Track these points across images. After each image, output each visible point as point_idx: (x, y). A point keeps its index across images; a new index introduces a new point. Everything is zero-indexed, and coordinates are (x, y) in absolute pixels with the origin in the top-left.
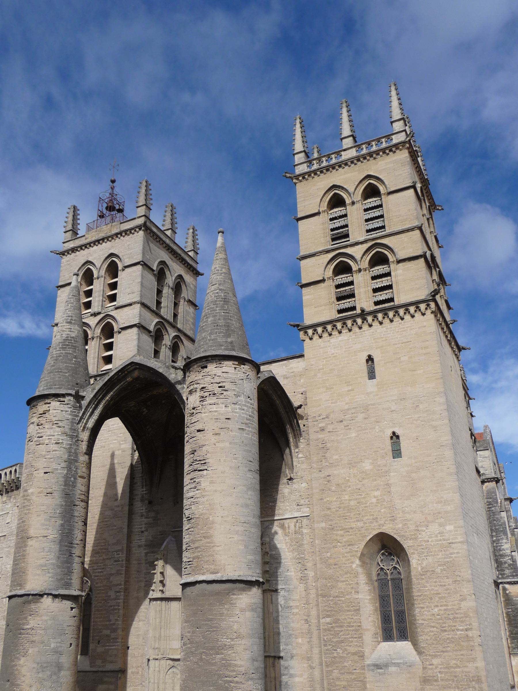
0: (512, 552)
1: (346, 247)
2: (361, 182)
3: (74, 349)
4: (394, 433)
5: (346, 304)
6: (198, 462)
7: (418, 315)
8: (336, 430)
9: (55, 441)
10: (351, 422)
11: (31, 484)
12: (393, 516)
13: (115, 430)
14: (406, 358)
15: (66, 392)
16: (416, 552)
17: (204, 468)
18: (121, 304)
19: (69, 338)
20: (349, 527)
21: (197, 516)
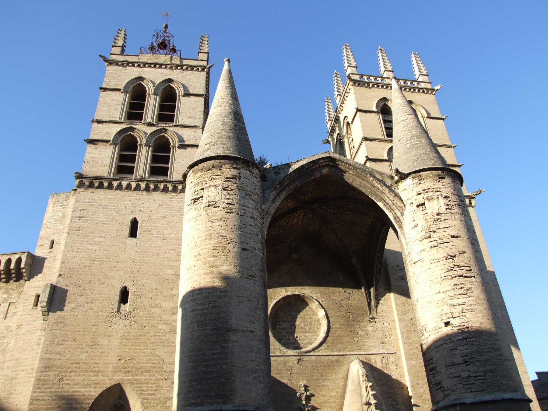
9: (250, 215)
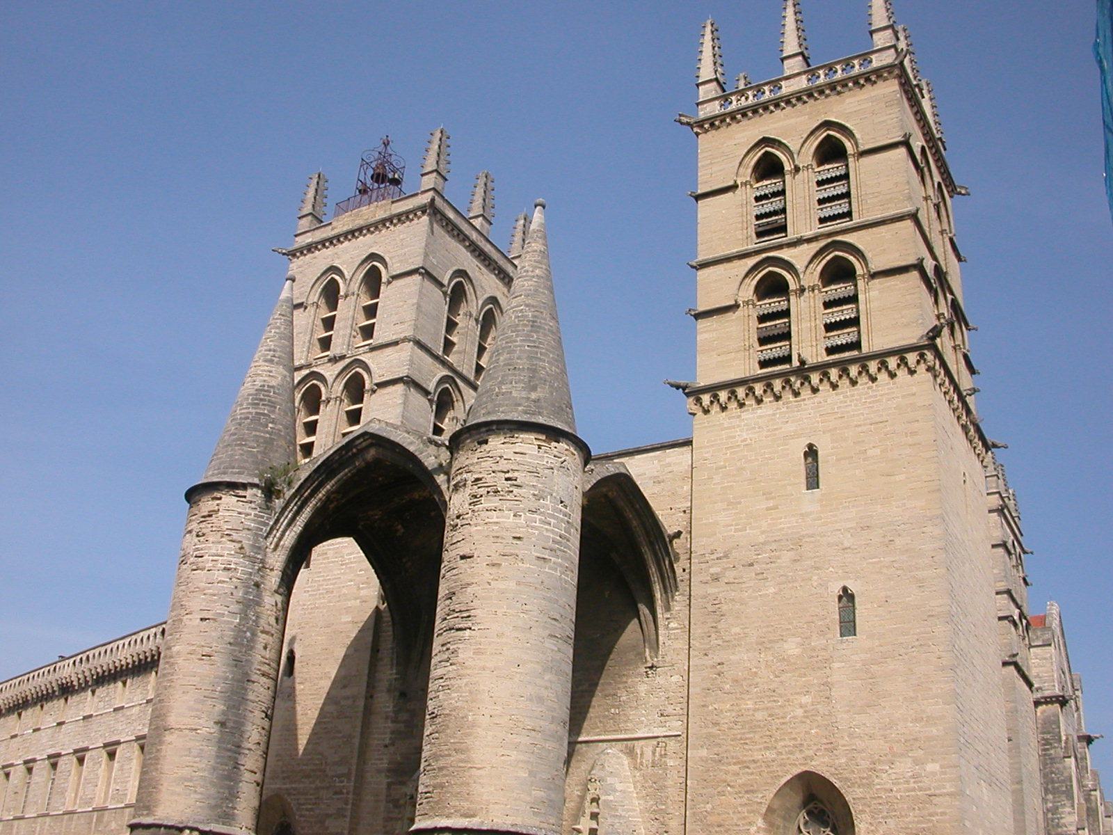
0: (1078, 829)
1: (780, 247)
2: (812, 133)
3: (272, 407)
4: (845, 589)
5: (776, 350)
6: (456, 615)
7: (902, 373)
8: (741, 581)
9: (223, 566)
10: (769, 566)
11: (178, 636)
12: (832, 743)
13: (351, 563)
14: (878, 451)
15: (250, 481)
16: (867, 810)
17: (466, 626)
18: (380, 341)
19: (266, 388)
20: (751, 759)
21: (448, 712)
